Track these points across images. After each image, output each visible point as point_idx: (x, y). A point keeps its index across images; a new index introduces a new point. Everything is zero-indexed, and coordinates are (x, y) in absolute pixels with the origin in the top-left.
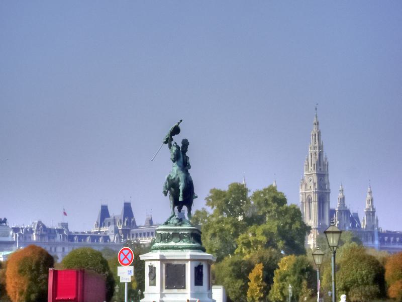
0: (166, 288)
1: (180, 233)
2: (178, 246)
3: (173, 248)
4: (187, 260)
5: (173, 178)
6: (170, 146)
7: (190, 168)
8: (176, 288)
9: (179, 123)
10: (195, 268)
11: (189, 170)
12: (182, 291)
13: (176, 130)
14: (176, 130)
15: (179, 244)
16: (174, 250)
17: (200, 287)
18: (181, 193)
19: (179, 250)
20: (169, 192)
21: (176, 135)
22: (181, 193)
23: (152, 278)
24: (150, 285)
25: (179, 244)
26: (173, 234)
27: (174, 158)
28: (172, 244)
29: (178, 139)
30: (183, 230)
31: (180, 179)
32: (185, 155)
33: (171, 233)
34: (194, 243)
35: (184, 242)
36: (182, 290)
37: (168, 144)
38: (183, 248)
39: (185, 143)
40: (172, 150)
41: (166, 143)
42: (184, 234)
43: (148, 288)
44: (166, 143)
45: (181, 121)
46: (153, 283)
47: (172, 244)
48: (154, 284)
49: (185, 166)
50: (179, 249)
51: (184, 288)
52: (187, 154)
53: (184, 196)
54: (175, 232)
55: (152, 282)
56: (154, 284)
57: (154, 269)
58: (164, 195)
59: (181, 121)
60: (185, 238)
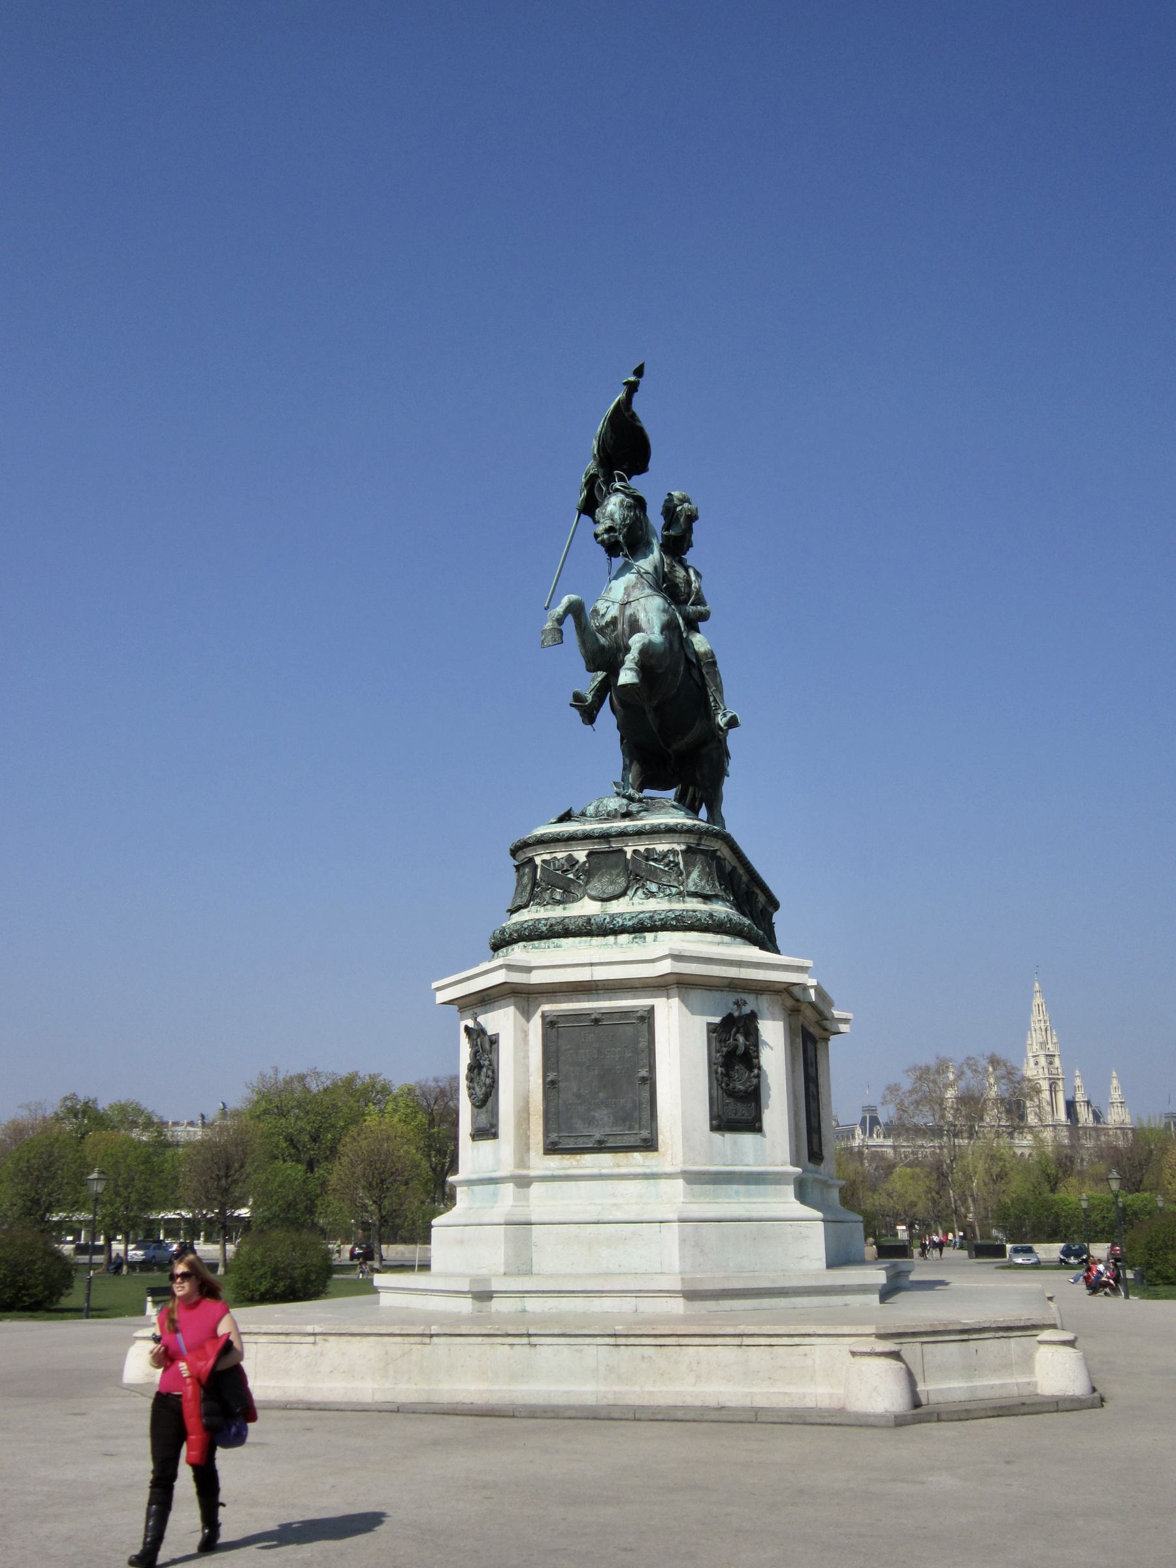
0: (551, 1149)
1: (629, 851)
2: (613, 917)
3: (589, 929)
5: (608, 618)
8: (600, 1147)
9: (632, 388)
10: (712, 1029)
12: (638, 1161)
16: (596, 940)
17: (747, 1139)
19: (624, 938)
23: (480, 1092)
28: (586, 908)
30: (639, 833)
31: (642, 617)
33: (581, 856)
34: (706, 898)
35: (650, 895)
36: (637, 1156)
38: (641, 927)
42: (649, 855)
43: (473, 1157)
45: (639, 372)
46: (486, 1131)
47: (586, 908)
51: (650, 1145)
54: (603, 847)
58: (576, 713)
59: (639, 372)
60: (653, 875)
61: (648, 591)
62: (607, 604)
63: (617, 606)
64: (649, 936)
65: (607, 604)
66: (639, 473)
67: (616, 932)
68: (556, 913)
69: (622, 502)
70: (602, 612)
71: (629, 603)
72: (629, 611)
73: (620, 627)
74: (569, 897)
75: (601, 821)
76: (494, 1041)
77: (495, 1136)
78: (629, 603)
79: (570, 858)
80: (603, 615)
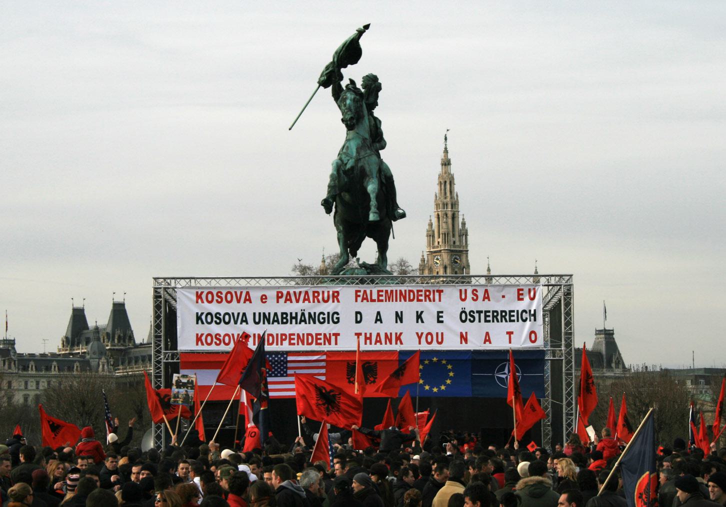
5: (348, 166)
6: (337, 94)
7: (383, 148)
9: (360, 33)
11: (381, 152)
13: (351, 52)
14: (351, 52)
18: (373, 202)
20: (334, 203)
21: (349, 66)
22: (373, 202)
27: (352, 118)
29: (353, 74)
31: (367, 169)
32: (371, 114)
37: (330, 88)
39: (373, 85)
40: (345, 100)
41: (324, 84)
44: (324, 84)
45: (367, 27)
49: (376, 139)
52: (377, 112)
53: (379, 208)
58: (322, 209)
59: (367, 27)
61: (368, 151)
62: (348, 158)
63: (353, 160)
65: (348, 158)
66: (352, 64)
69: (354, 99)
70: (345, 162)
71: (360, 159)
72: (360, 165)
73: (355, 172)
78: (360, 159)
80: (346, 164)
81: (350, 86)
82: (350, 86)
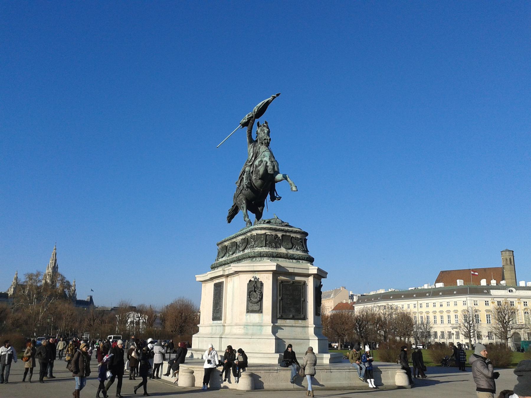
4: (308, 275)
15: (291, 252)
16: (288, 260)
19: (294, 261)
24: (249, 311)
25: (291, 252)
26: (283, 236)
28: (282, 250)
33: (280, 235)
35: (297, 249)
45: (278, 95)
47: (282, 250)
48: (260, 311)
50: (294, 258)
55: (257, 307)
56: (260, 311)
57: (259, 286)
59: (278, 95)
64: (301, 261)
67: (292, 259)
68: (274, 250)
74: (276, 247)
75: (282, 226)
76: (262, 284)
77: (262, 312)
79: (276, 235)
81: (265, 125)
82: (265, 125)
